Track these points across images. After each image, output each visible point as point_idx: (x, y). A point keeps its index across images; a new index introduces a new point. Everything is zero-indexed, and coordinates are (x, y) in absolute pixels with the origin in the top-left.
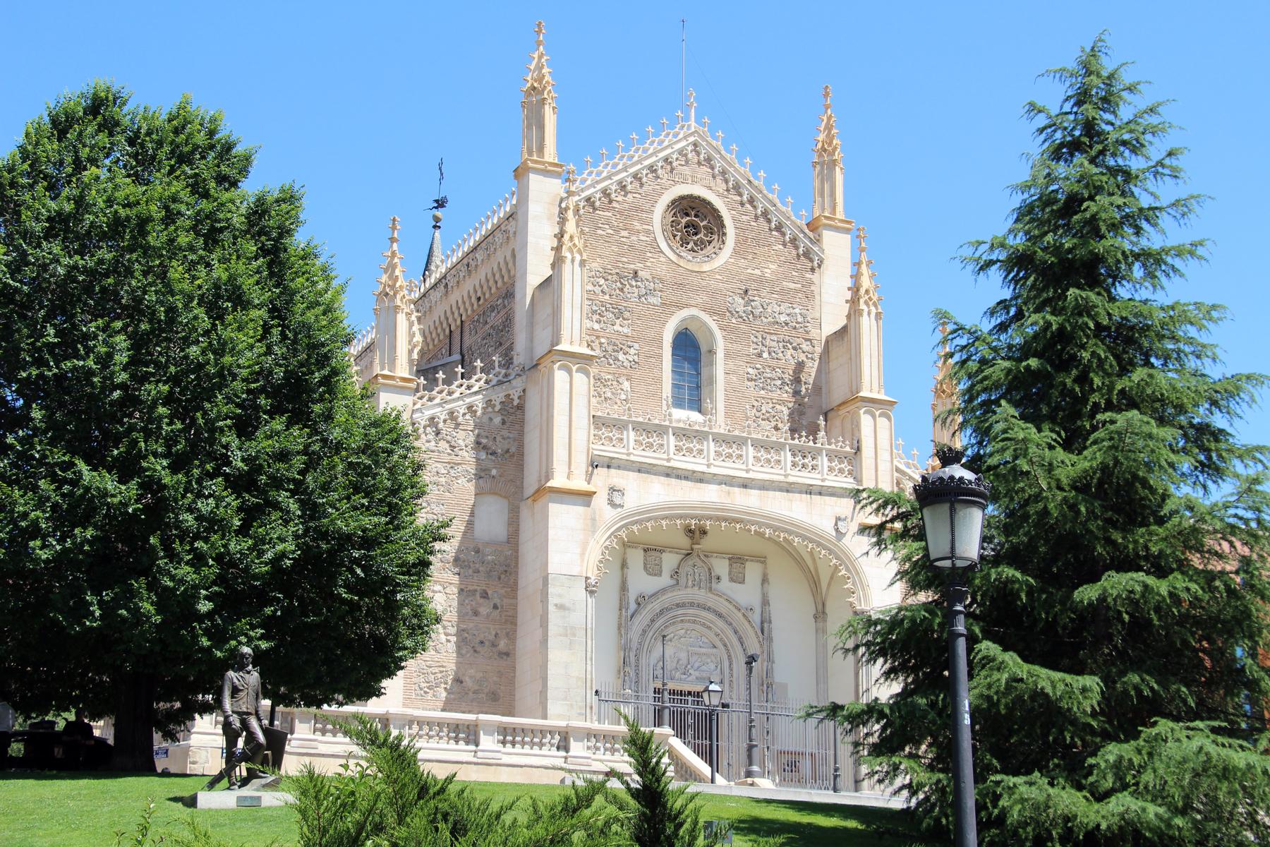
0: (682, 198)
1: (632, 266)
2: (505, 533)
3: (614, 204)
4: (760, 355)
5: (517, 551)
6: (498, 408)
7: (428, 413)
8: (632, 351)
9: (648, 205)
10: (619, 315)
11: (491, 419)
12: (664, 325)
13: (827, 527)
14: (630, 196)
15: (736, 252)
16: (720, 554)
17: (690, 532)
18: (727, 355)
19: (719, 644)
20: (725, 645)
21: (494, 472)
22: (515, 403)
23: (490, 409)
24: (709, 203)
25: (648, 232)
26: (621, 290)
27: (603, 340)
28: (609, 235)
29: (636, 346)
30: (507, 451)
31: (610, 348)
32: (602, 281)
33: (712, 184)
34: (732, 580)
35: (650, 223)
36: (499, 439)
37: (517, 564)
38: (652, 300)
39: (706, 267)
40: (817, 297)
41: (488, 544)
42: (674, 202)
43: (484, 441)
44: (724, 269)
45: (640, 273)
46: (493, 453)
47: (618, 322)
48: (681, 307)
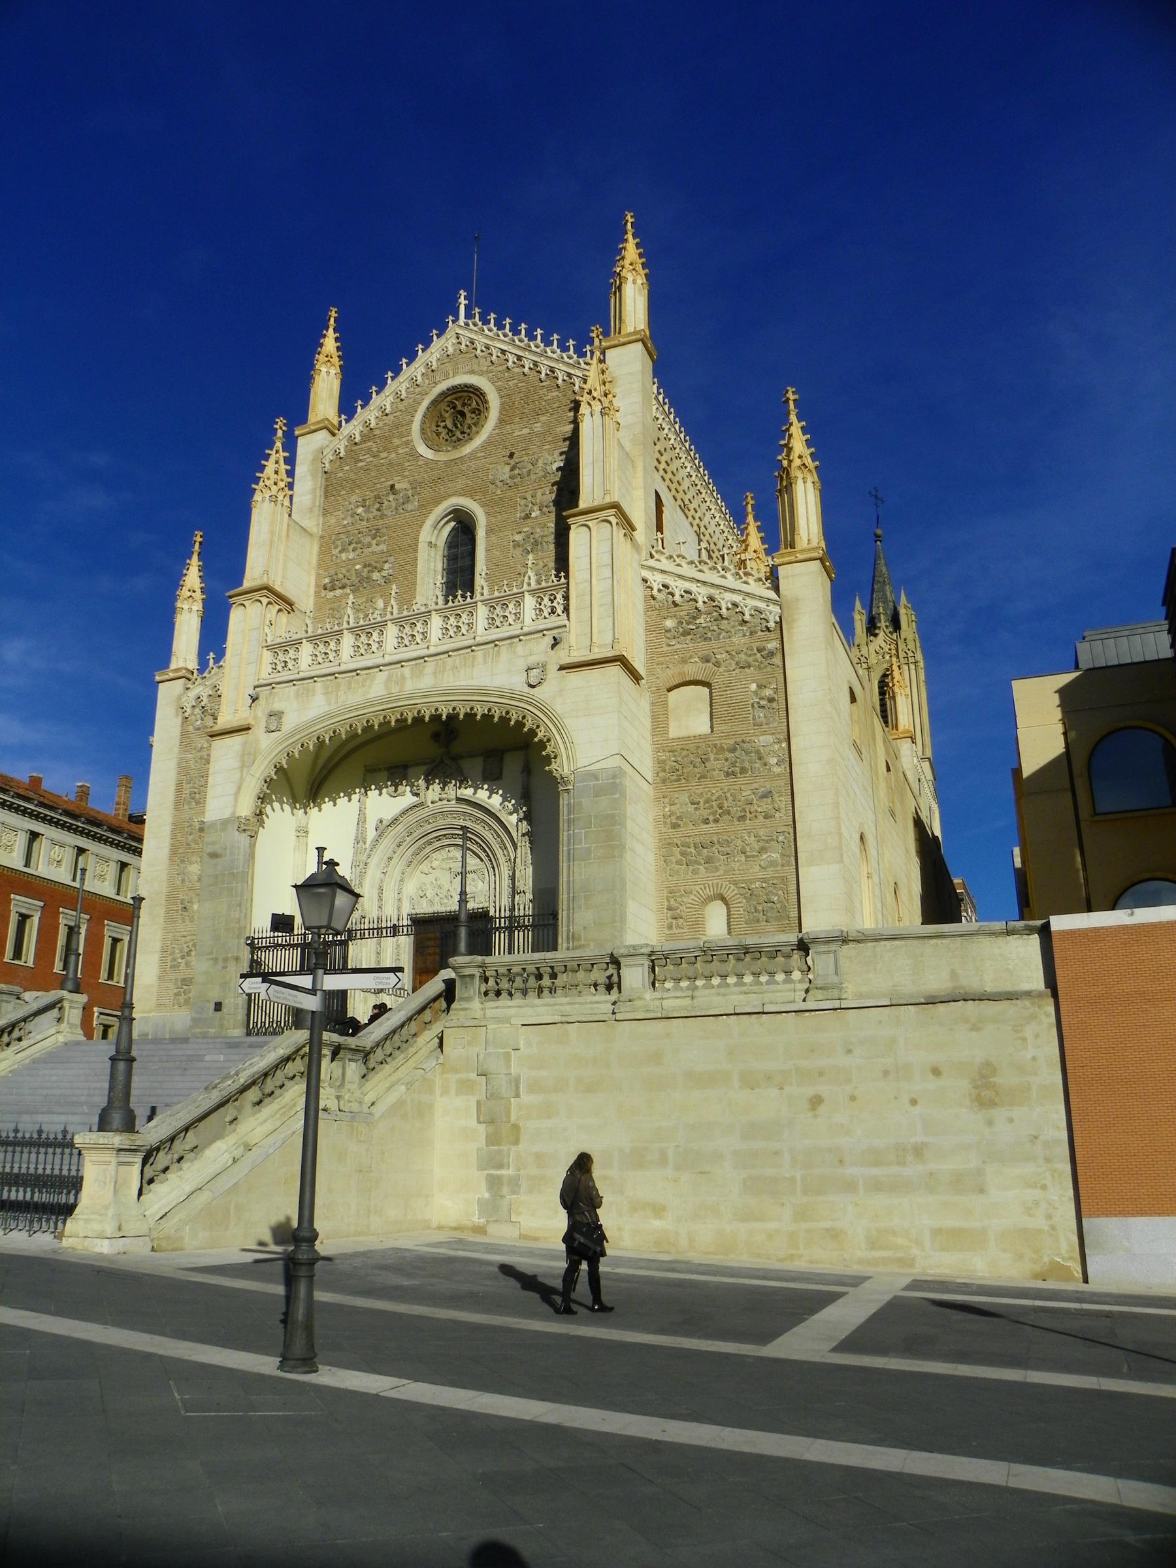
0: (444, 395)
1: (391, 483)
3: (377, 432)
4: (528, 516)
7: (192, 694)
8: (386, 566)
10: (376, 534)
12: (421, 526)
13: (517, 683)
14: (391, 417)
15: (502, 422)
16: (472, 756)
17: (436, 736)
18: (489, 532)
19: (483, 855)
20: (488, 856)
24: (471, 386)
25: (407, 443)
26: (378, 510)
27: (358, 567)
28: (368, 464)
29: (391, 559)
31: (365, 574)
32: (360, 510)
33: (476, 368)
34: (485, 779)
35: (409, 434)
38: (409, 507)
39: (467, 449)
42: (434, 403)
44: (483, 447)
45: (397, 487)
47: (374, 542)
48: (437, 502)
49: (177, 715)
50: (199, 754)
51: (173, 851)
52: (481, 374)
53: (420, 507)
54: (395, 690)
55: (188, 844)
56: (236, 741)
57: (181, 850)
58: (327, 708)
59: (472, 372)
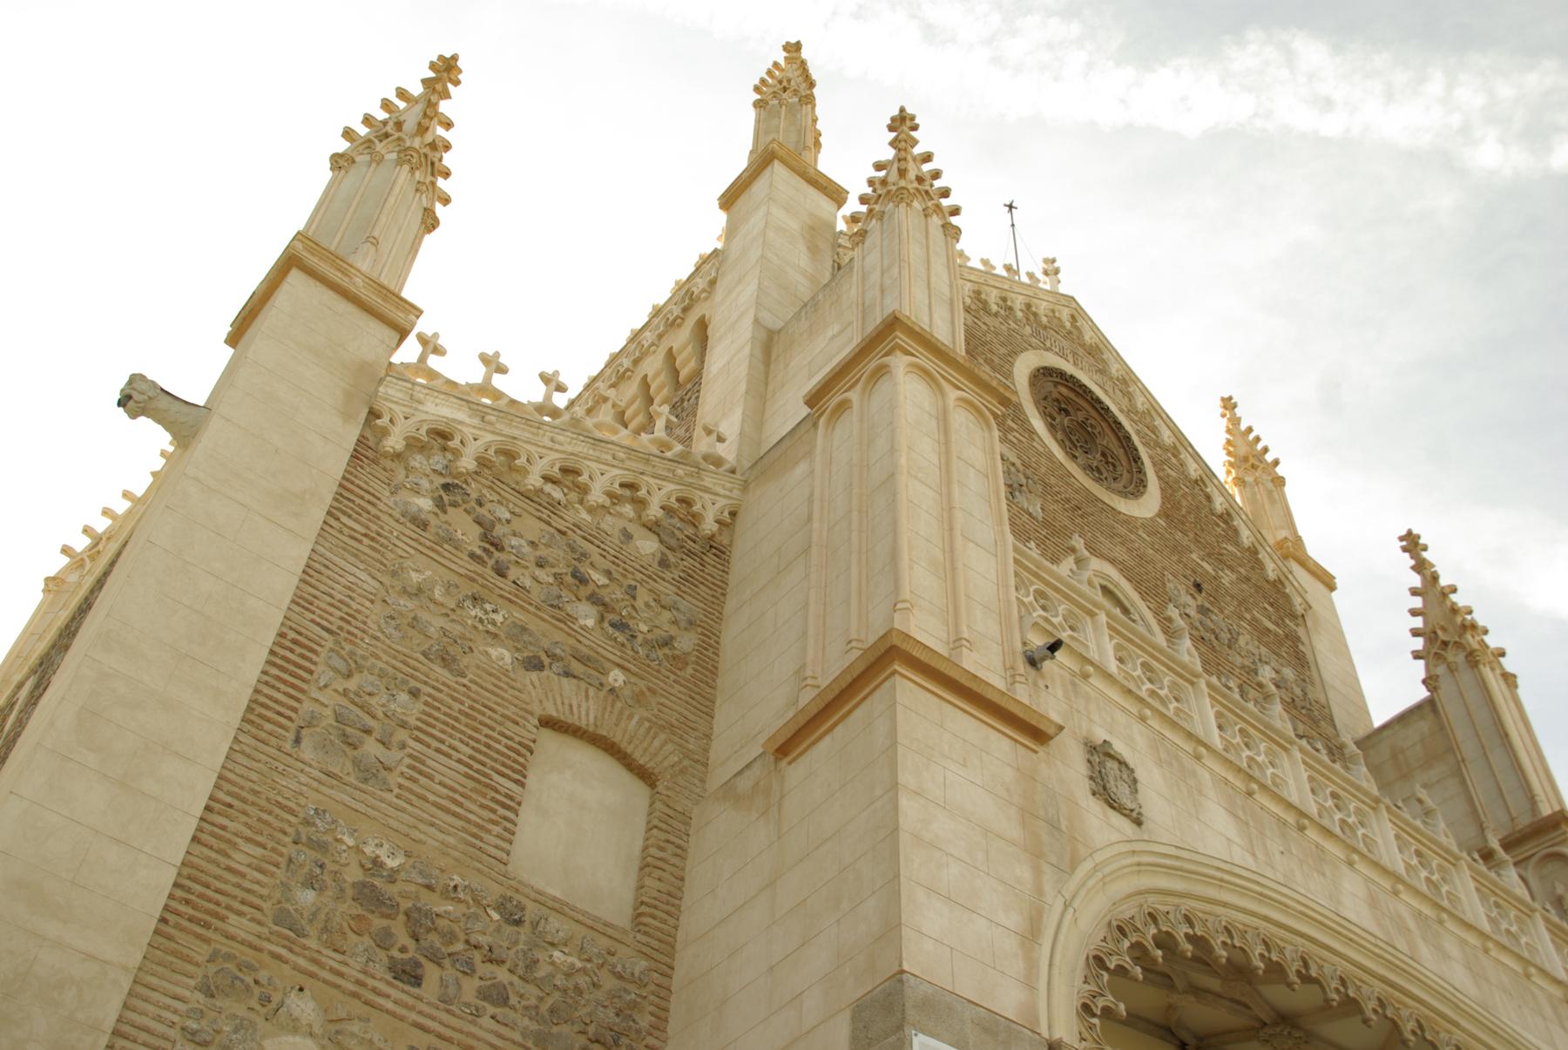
2: (627, 897)
5: (667, 971)
6: (654, 511)
9: (1003, 351)
11: (628, 536)
15: (1164, 513)
21: (616, 677)
22: (709, 526)
23: (628, 510)
30: (667, 642)
35: (1009, 375)
36: (643, 596)
37: (661, 1017)
39: (1124, 506)
40: (1313, 668)
41: (560, 908)
43: (598, 578)
46: (620, 626)
49: (347, 417)
50: (406, 604)
51: (192, 904)
52: (1121, 411)
53: (1046, 524)
54: (1401, 944)
55: (282, 918)
56: (1000, 745)
57: (238, 925)
58: (1250, 862)
59: (1106, 392)
